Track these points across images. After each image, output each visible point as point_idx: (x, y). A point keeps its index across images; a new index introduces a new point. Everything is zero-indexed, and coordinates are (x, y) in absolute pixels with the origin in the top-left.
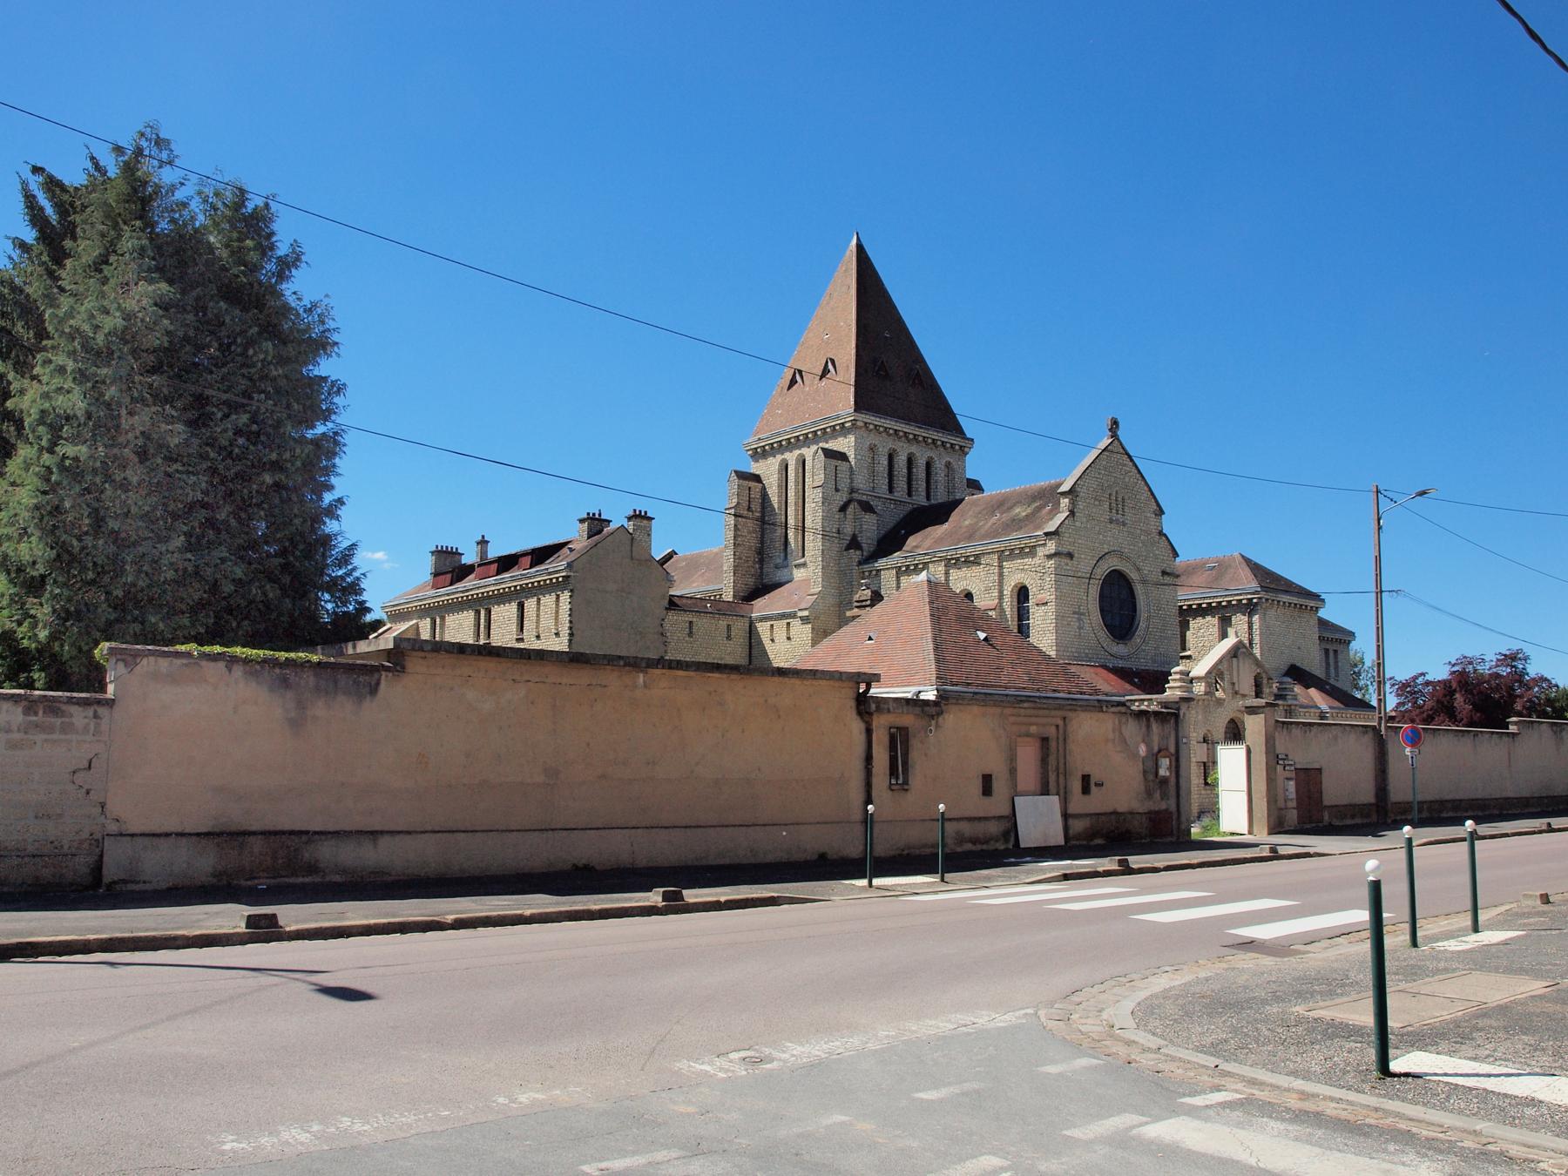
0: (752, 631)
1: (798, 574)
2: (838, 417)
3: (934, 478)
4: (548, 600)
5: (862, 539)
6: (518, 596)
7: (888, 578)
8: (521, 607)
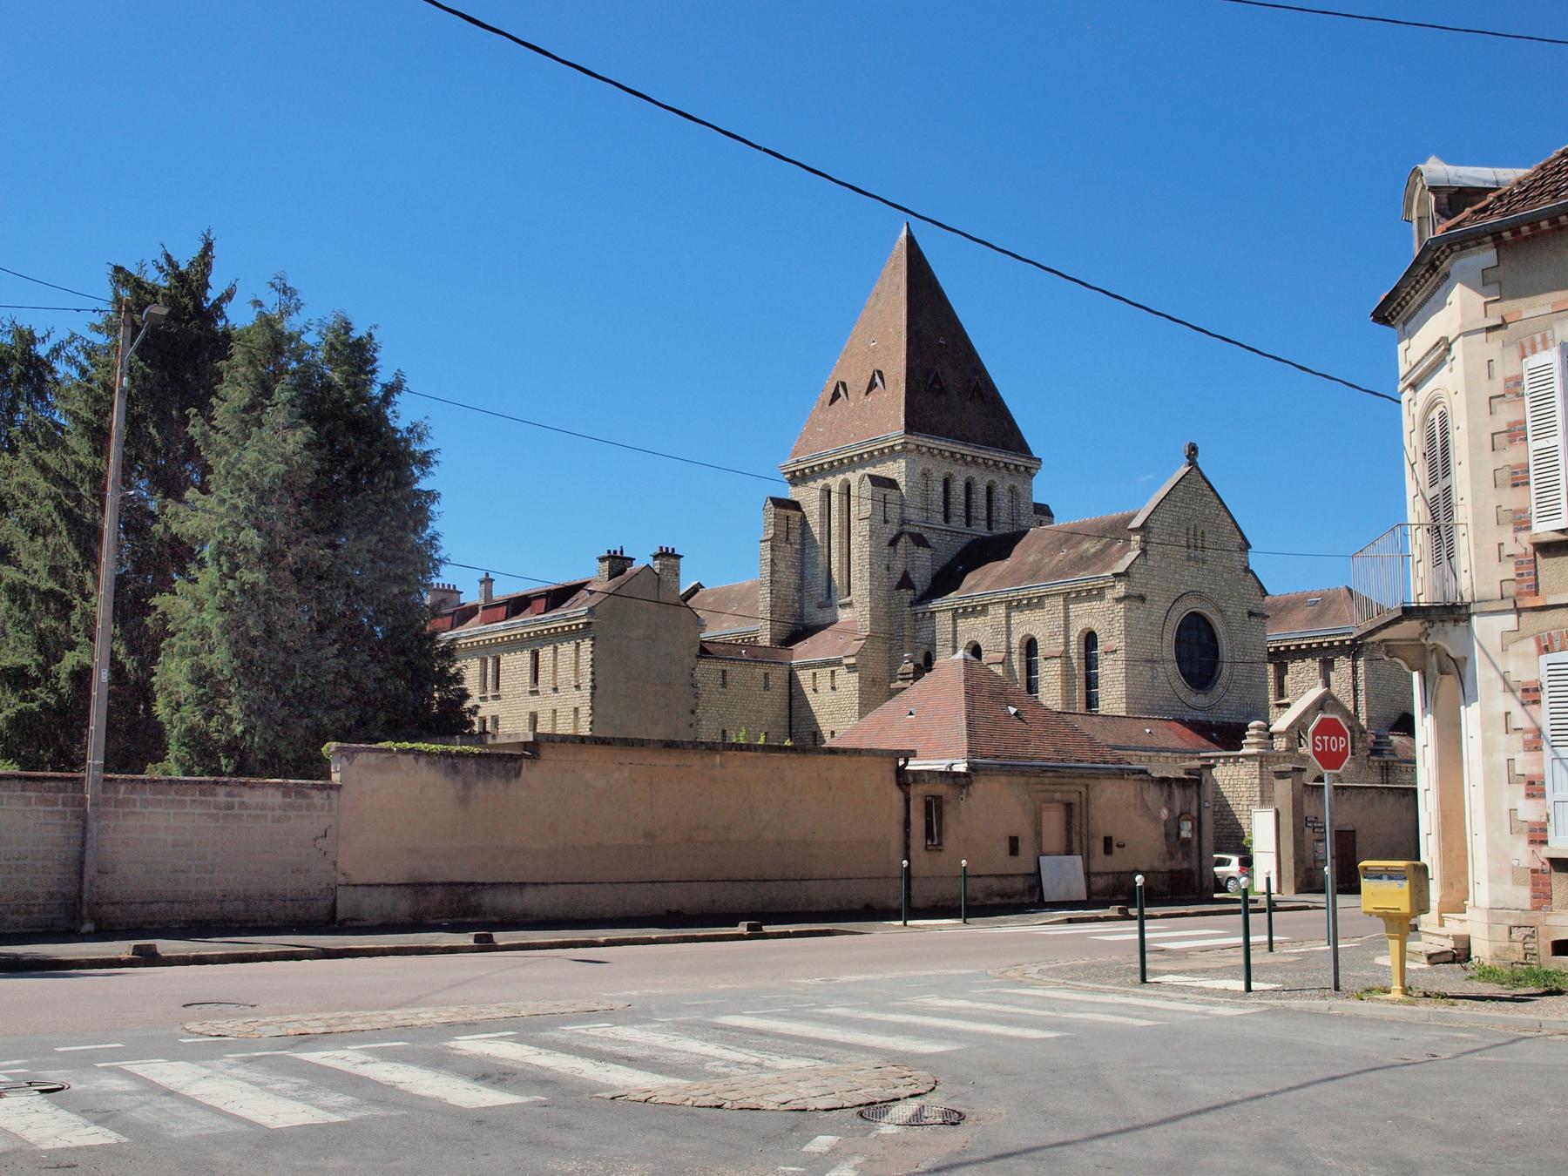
0: (792, 679)
1: (844, 615)
2: (887, 439)
3: (995, 505)
4: (567, 649)
5: (915, 577)
6: (532, 644)
7: (943, 622)
8: (535, 655)
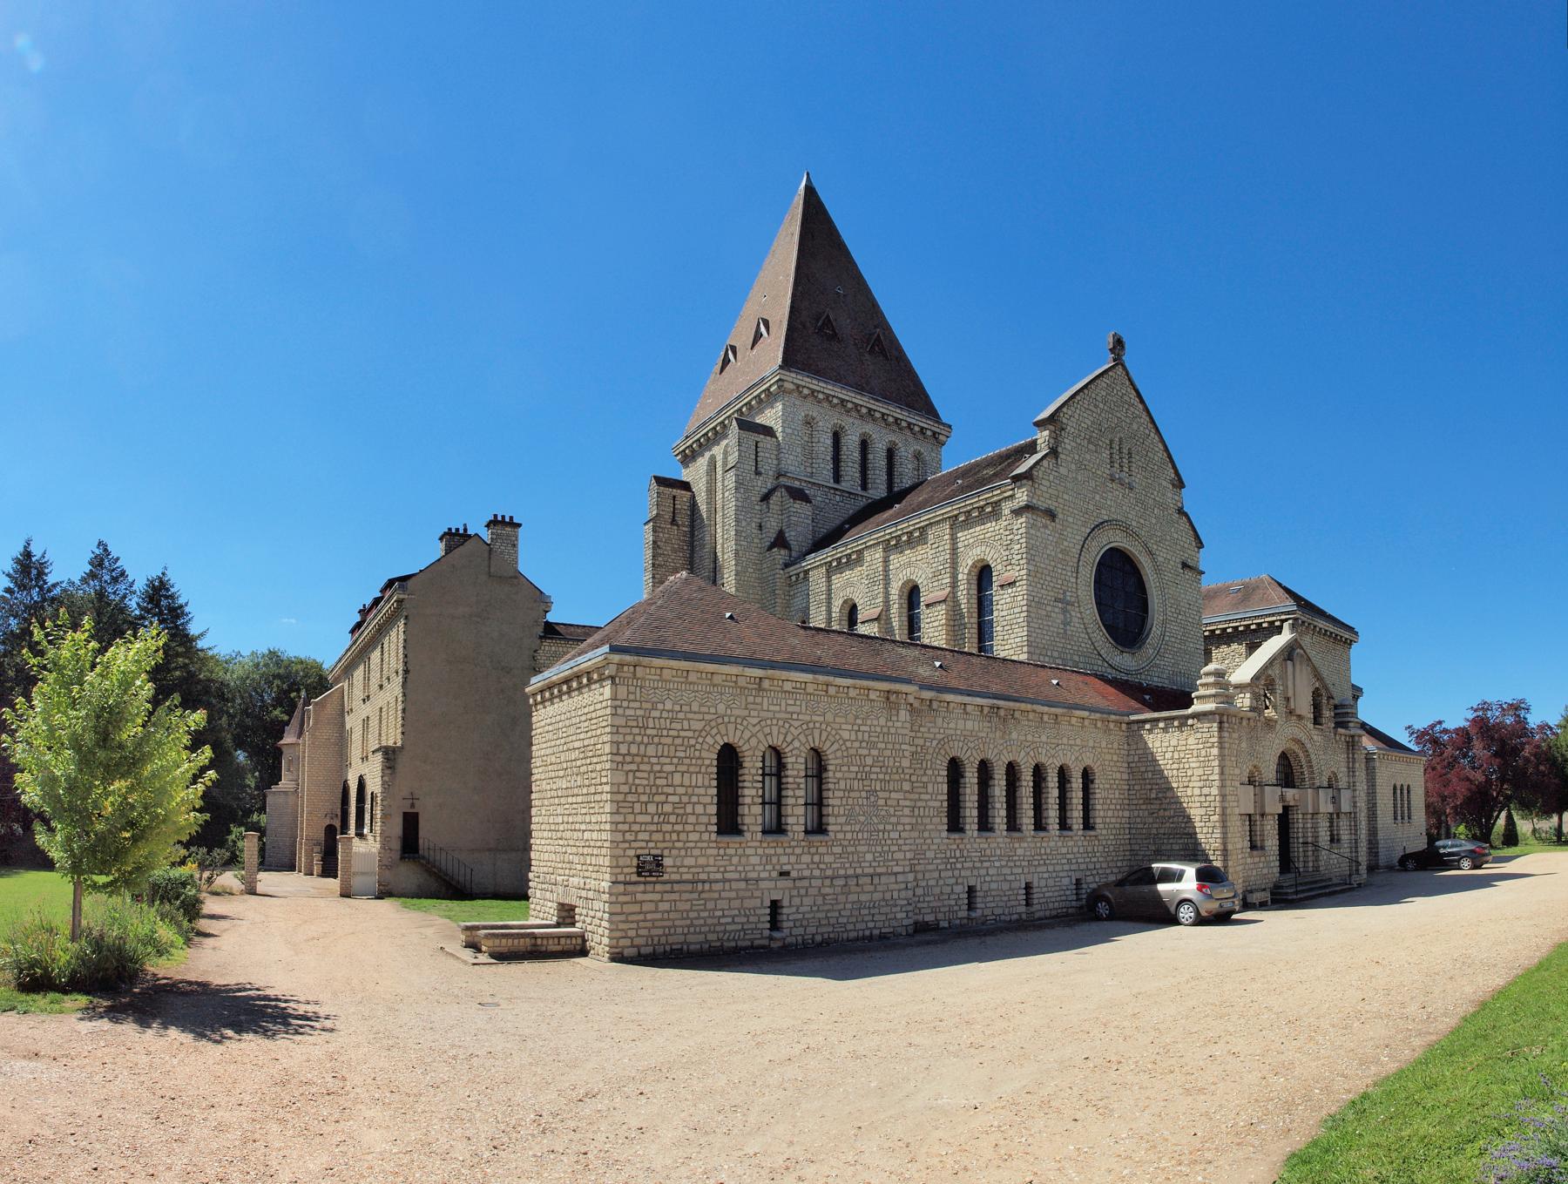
3: (897, 469)
5: (790, 535)
7: (817, 579)
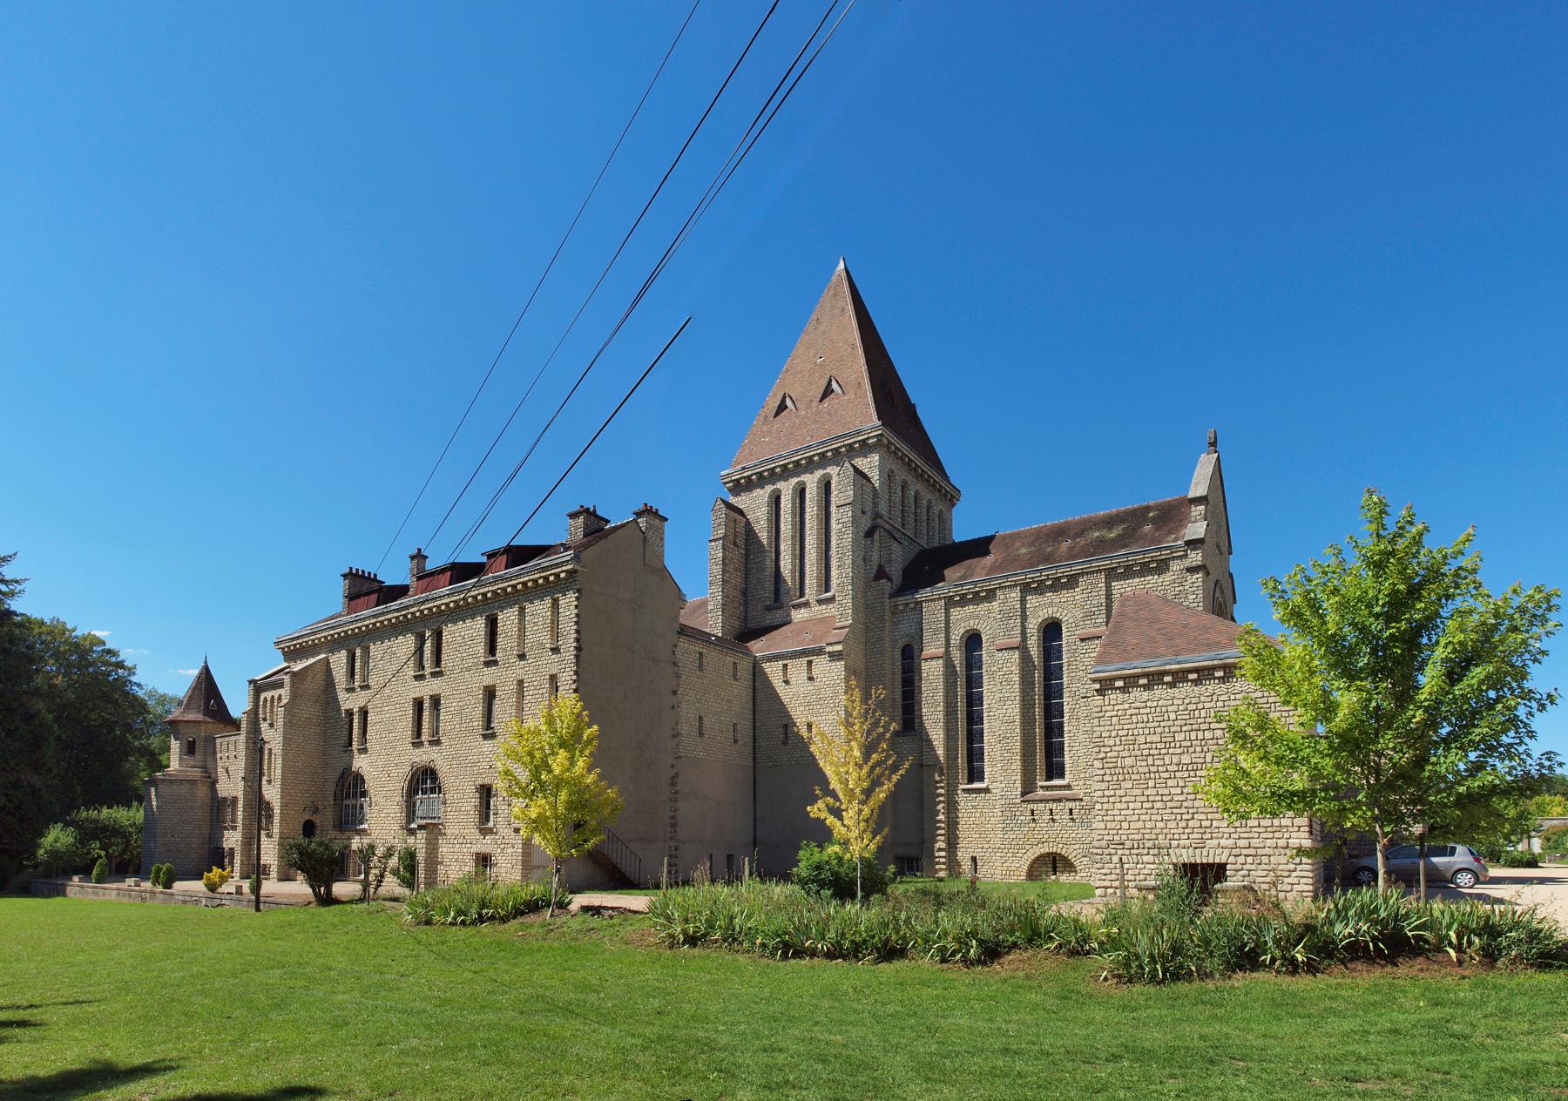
0: (757, 673)
1: (798, 616)
2: (858, 433)
6: (489, 610)
7: (933, 613)
8: (492, 624)
